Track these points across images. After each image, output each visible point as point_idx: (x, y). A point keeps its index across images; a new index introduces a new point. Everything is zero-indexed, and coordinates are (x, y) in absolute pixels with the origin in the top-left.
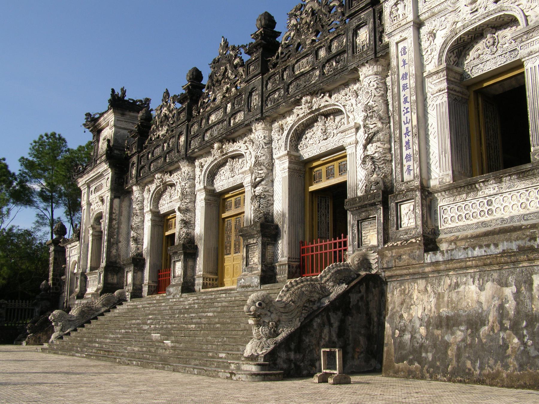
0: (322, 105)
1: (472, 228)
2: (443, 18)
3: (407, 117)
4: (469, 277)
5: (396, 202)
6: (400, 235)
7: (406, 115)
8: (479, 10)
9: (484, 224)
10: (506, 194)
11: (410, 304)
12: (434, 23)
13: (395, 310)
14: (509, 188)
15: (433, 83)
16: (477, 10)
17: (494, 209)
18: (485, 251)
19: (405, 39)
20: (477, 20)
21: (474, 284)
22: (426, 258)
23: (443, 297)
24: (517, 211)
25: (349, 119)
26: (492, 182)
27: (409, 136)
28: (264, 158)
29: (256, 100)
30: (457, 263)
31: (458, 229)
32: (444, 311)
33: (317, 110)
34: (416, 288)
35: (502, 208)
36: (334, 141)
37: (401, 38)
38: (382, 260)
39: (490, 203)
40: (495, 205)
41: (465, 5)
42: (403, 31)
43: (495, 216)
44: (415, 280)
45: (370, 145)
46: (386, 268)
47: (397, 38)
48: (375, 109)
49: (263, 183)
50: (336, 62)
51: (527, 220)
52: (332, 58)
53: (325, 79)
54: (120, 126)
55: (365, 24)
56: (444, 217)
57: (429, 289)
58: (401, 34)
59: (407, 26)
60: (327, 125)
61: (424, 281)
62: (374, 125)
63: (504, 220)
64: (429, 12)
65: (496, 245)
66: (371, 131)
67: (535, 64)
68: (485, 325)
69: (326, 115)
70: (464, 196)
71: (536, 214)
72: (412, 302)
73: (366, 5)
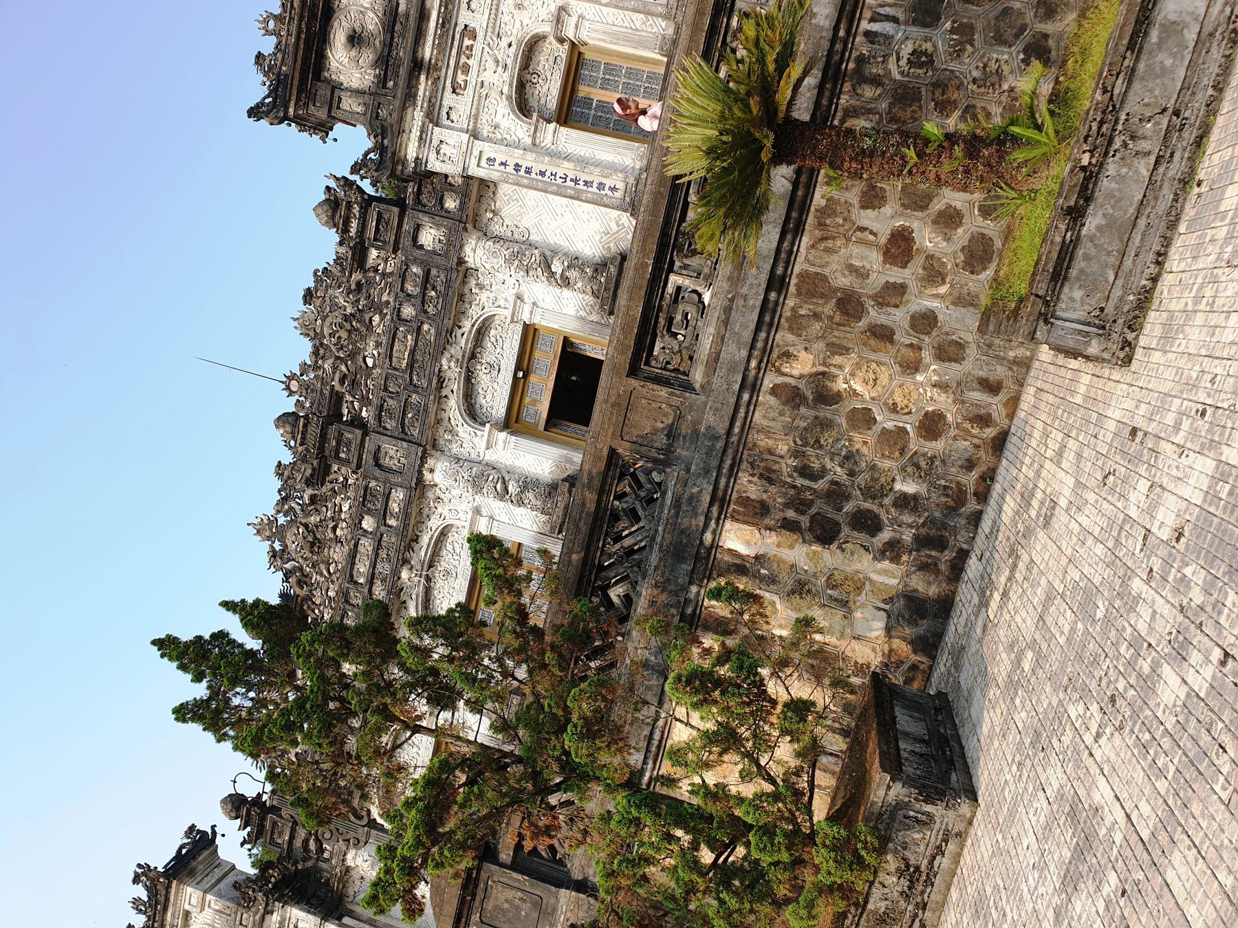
0: (463, 342)
2: (486, 109)
7: (557, 178)
12: (484, 120)
28: (475, 469)
29: (394, 453)
33: (463, 356)
42: (471, 153)
45: (553, 266)
47: (474, 162)
48: (516, 250)
49: (507, 479)
50: (433, 289)
52: (424, 295)
54: (209, 884)
55: (418, 228)
60: (484, 361)
66: (538, 262)
69: (473, 356)
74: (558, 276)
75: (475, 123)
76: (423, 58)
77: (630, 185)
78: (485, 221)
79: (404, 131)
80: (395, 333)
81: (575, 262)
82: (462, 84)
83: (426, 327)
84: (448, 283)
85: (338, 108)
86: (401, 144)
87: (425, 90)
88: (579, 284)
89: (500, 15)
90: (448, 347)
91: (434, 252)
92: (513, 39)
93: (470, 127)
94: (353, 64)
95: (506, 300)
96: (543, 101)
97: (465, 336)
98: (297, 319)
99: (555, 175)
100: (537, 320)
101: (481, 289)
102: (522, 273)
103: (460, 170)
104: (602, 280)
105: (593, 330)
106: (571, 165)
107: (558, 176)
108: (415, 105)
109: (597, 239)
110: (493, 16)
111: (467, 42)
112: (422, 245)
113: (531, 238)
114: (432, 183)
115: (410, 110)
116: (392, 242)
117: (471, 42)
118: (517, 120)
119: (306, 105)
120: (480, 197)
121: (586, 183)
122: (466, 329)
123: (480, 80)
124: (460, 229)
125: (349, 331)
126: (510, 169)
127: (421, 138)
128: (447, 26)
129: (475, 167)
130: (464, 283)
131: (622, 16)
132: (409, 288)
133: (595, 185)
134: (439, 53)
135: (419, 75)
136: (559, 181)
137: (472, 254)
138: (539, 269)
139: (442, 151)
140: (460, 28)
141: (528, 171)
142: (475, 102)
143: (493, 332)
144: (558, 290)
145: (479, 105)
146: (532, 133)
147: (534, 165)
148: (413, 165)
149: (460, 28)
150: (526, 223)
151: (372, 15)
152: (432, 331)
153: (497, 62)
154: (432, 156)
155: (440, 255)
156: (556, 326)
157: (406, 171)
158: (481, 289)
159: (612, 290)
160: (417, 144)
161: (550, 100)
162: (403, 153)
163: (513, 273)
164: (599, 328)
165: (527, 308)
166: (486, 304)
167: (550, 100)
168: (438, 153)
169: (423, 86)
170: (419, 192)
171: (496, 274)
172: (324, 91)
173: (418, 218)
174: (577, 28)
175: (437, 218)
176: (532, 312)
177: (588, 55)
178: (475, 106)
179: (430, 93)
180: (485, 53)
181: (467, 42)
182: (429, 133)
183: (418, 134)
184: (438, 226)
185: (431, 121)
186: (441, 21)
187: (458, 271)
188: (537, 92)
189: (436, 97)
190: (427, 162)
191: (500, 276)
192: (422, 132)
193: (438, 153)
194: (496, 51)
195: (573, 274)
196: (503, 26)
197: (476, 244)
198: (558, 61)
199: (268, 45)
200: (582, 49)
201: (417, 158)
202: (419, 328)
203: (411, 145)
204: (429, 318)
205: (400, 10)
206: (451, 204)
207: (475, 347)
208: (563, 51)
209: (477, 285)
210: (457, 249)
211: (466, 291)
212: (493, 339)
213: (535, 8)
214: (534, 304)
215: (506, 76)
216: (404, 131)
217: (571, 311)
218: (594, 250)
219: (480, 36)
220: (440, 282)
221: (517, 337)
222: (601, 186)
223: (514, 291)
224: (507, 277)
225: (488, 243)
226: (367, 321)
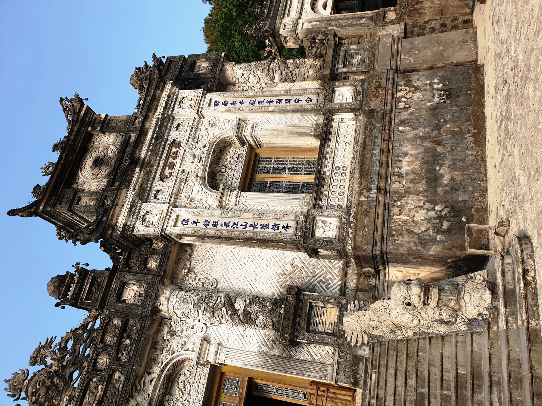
1: (353, 182)
2: (185, 189)
3: (241, 225)
4: (395, 165)
5: (310, 237)
6: (343, 235)
8: (202, 156)
9: (352, 172)
10: (336, 155)
11: (412, 223)
12: (183, 196)
13: (417, 241)
14: (332, 152)
15: (227, 203)
16: (201, 158)
17: (344, 165)
18: (378, 146)
19: (178, 216)
20: (207, 161)
21: (401, 161)
22: (372, 199)
23: (409, 187)
24: (350, 148)
25: (190, 349)
26: (324, 161)
27: (257, 224)
30: (381, 171)
31: (350, 194)
32: (421, 187)
34: (397, 217)
35: (343, 159)
36: (195, 401)
37: (174, 221)
38: (364, 250)
39: (338, 168)
40: (341, 165)
41: (192, 162)
43: (348, 166)
44: (390, 218)
45: (236, 304)
46: (373, 248)
47: (171, 223)
50: (128, 338)
51: (358, 141)
53: (133, 360)
55: (123, 286)
56: (336, 208)
57: (399, 203)
58: (170, 220)
59: (169, 212)
61: (392, 209)
62: (219, 298)
63: (354, 157)
64: (173, 197)
65: (376, 137)
66: (223, 302)
67: (260, 128)
68: (436, 149)
70: (325, 187)
71: (356, 135)
72: (410, 220)
73: (109, 278)
74: (241, 312)
75: (176, 198)
76: (139, 158)
77: (300, 222)
78: (181, 277)
79: (117, 205)
80: (88, 384)
81: (255, 300)
82: (168, 175)
83: (117, 375)
84: (141, 332)
85: (77, 204)
86: (113, 215)
87: (138, 178)
88: (261, 319)
89: (199, 131)
90: (135, 394)
91: (134, 304)
92: (207, 142)
93: (172, 201)
94: (94, 177)
95: (194, 343)
96: (229, 183)
97: (153, 383)
98: (9, 380)
99: (237, 224)
100: (221, 359)
101: (172, 335)
102: (208, 315)
103: (159, 230)
104: (282, 311)
105: (275, 364)
106: (250, 215)
107: (239, 225)
108: (128, 187)
109: (275, 280)
110: (193, 132)
111: (174, 150)
112: (125, 300)
113: (219, 286)
114: (140, 250)
115: (124, 191)
116: (99, 300)
117: (177, 149)
118: (208, 192)
119: (54, 205)
120: (178, 260)
121: (263, 226)
122: (155, 375)
123: (181, 169)
124: (158, 282)
125: (48, 388)
126: (201, 225)
127: (130, 210)
128: (160, 140)
129: (172, 228)
130: (159, 331)
131: (285, 119)
132: (109, 339)
133: (270, 226)
134: (152, 155)
135: (135, 168)
136: (240, 228)
137: (165, 303)
138: (224, 309)
139: (147, 220)
140: (169, 142)
141: (215, 224)
142: (177, 184)
143: (182, 378)
144: (241, 328)
145: (179, 187)
146: (219, 198)
147: (220, 219)
148: (121, 229)
149: (169, 142)
150: (215, 274)
151: (112, 147)
152: (122, 379)
153: (194, 156)
154: (139, 223)
155: (138, 306)
156: (239, 365)
157: (115, 235)
158: (172, 335)
159: (291, 317)
160: (126, 214)
161: (235, 182)
162: (114, 221)
163: (200, 317)
164: (282, 361)
165: (213, 348)
166: (176, 349)
167: (235, 182)
168: (143, 221)
169: (137, 175)
170: (129, 258)
171: (187, 320)
172: (69, 194)
173: (124, 277)
174: (252, 129)
175: (139, 275)
176: (217, 352)
177: (263, 154)
178: (176, 187)
179: (142, 180)
180: (186, 152)
181: (174, 150)
182: (138, 208)
183: (129, 207)
184: (139, 282)
185: (140, 199)
186: (155, 135)
187: (153, 320)
188: (225, 178)
189: (147, 184)
190: (133, 228)
191: (190, 322)
192: (132, 206)
193: (143, 221)
194: (194, 151)
195: (254, 309)
196: (200, 138)
197: (170, 294)
198: (241, 157)
199: (44, 181)
200: (258, 151)
201: (125, 225)
202: (111, 377)
203: (122, 215)
204: (120, 365)
205: (131, 140)
206: (152, 264)
207: (164, 395)
208: (244, 151)
209: (169, 332)
210: (152, 298)
211: (159, 338)
212: (181, 386)
213: (223, 124)
214: (220, 344)
215: (201, 165)
216: (117, 205)
217: (254, 347)
218: (273, 290)
219: (183, 145)
220: (135, 331)
221: (204, 381)
222: (275, 227)
223: (202, 335)
224: (196, 323)
225: (181, 293)
226: (67, 376)
